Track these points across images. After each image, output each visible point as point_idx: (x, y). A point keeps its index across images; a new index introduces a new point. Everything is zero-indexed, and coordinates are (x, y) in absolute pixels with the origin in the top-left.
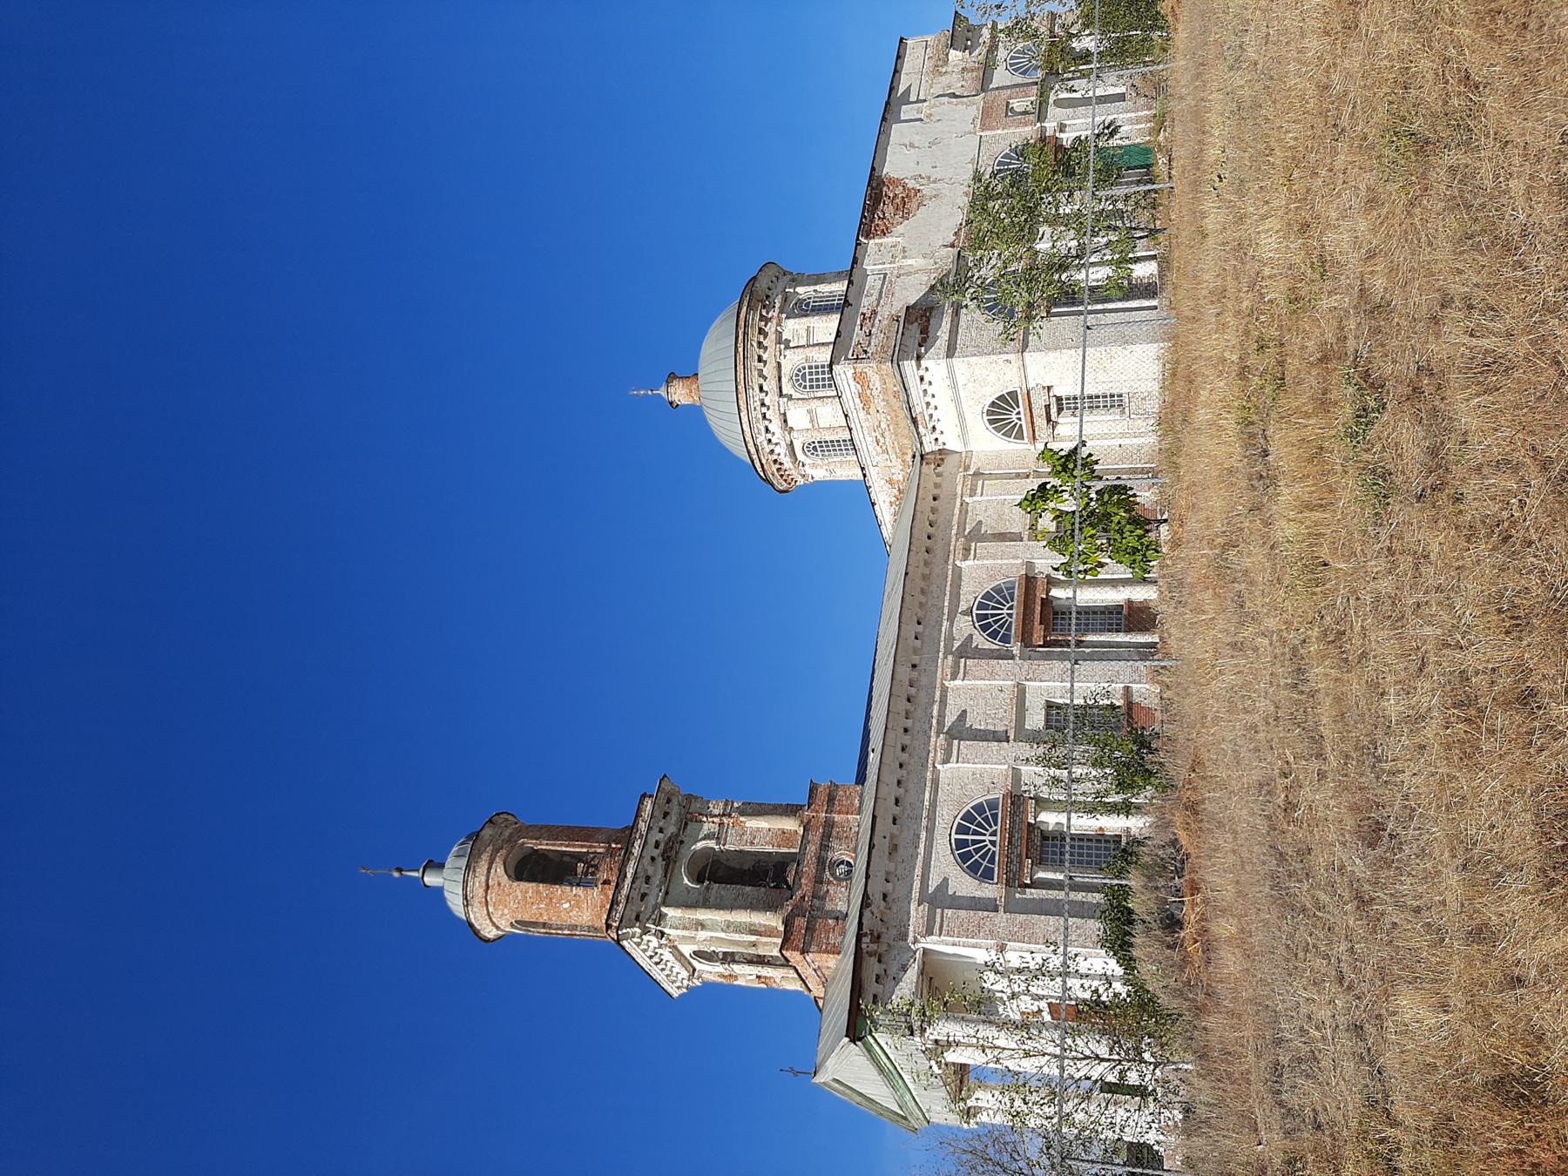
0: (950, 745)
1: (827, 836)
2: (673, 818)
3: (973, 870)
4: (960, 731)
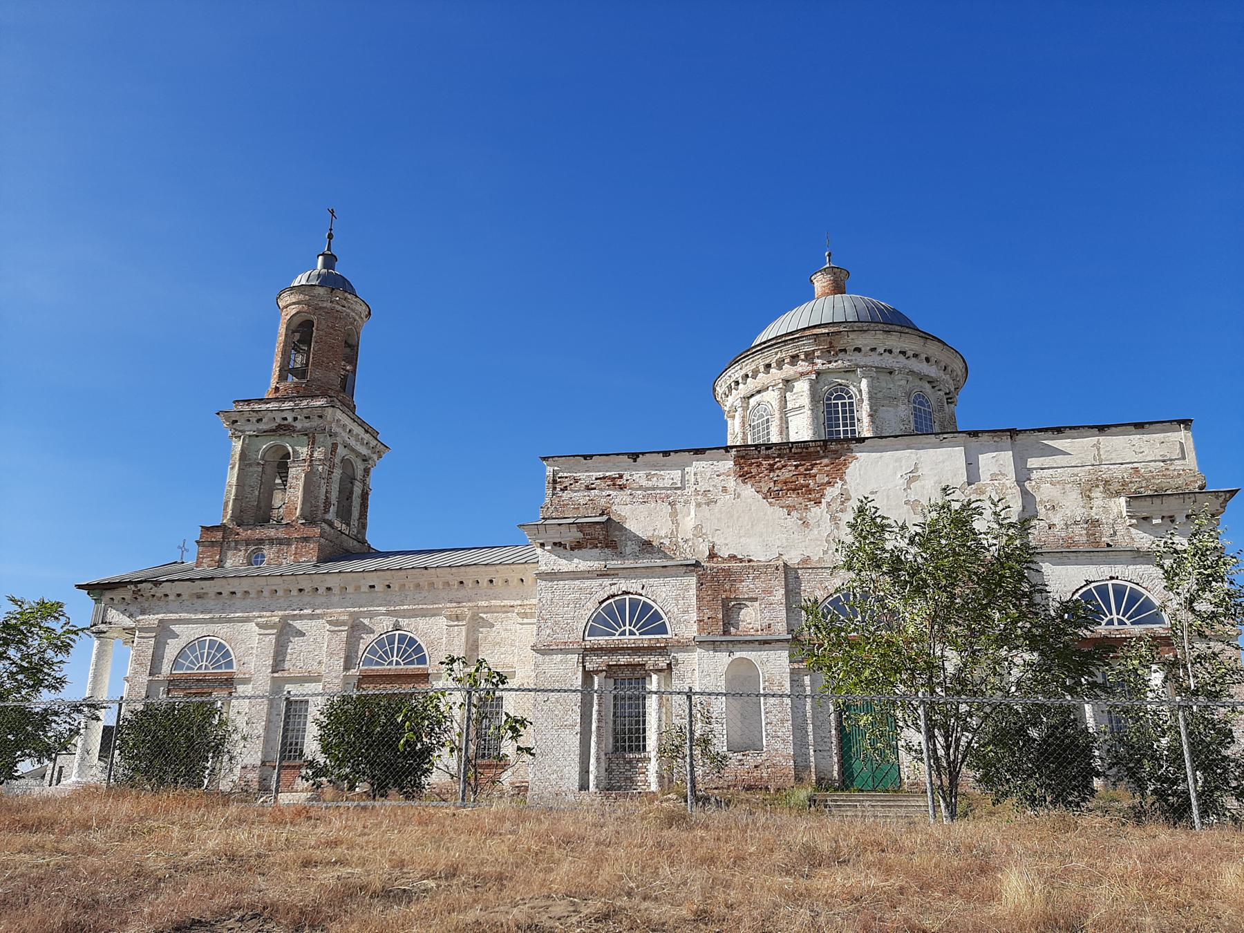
0: (272, 627)
1: (280, 542)
2: (307, 424)
3: (181, 653)
4: (285, 633)
